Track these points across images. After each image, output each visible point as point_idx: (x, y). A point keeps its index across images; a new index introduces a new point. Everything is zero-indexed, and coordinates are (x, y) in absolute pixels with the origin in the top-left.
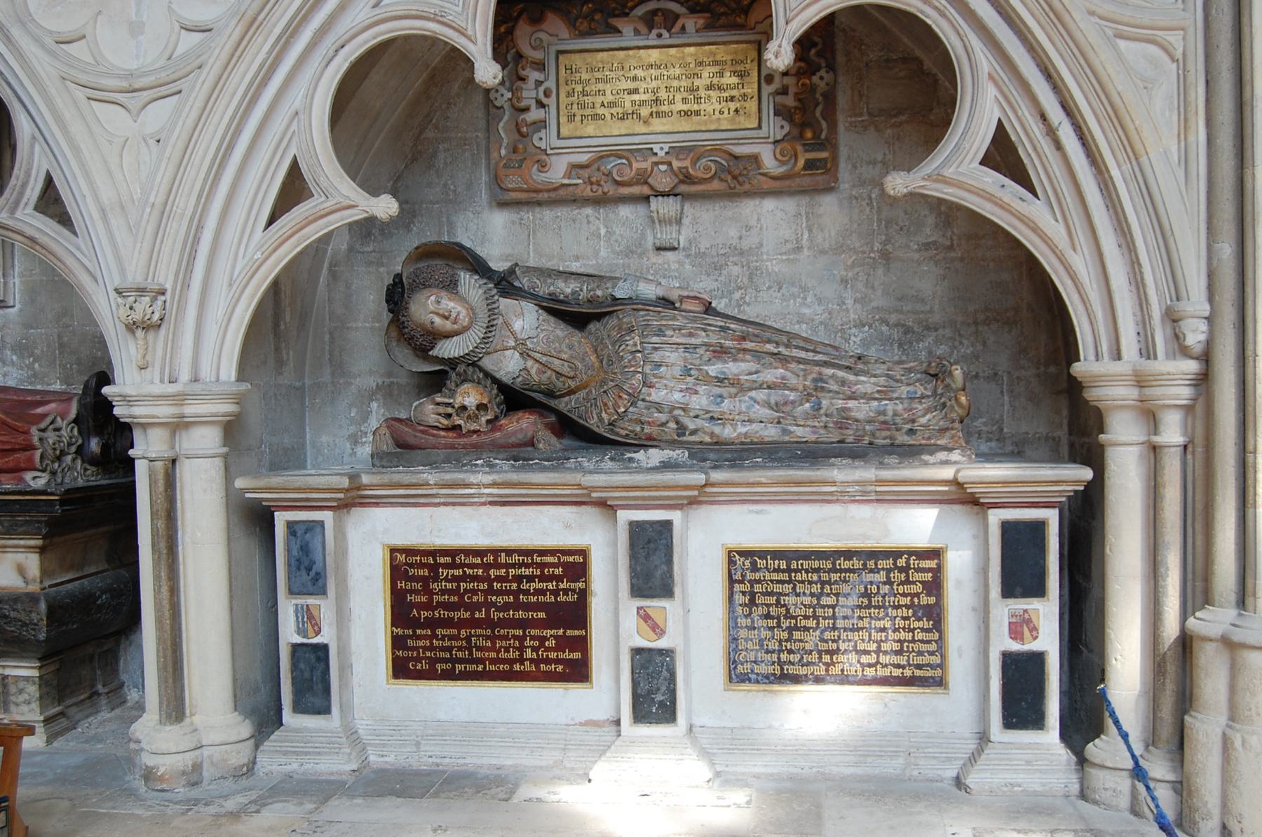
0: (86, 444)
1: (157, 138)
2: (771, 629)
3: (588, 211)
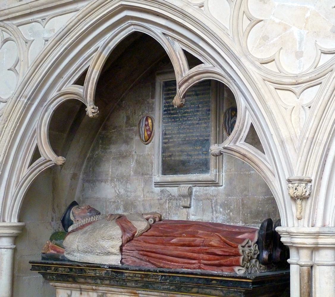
0: (261, 254)
1: (309, 106)
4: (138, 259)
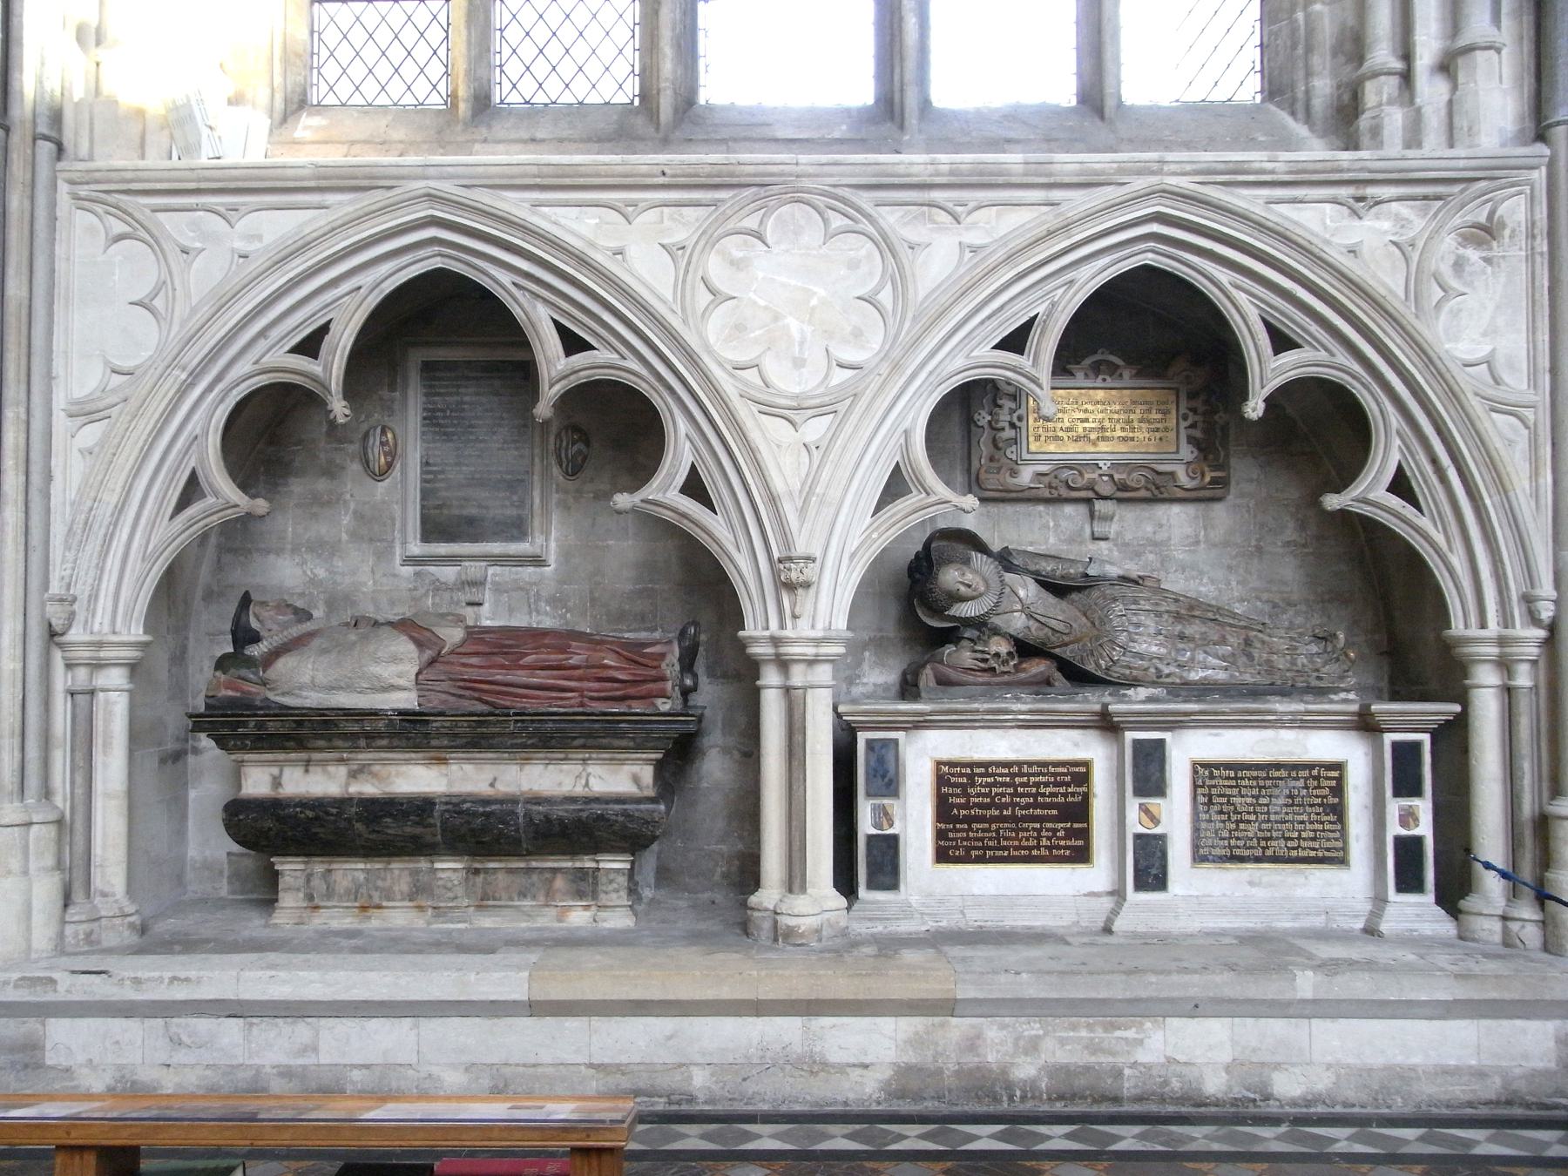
2: (1224, 822)
3: (1041, 508)
4: (454, 695)
